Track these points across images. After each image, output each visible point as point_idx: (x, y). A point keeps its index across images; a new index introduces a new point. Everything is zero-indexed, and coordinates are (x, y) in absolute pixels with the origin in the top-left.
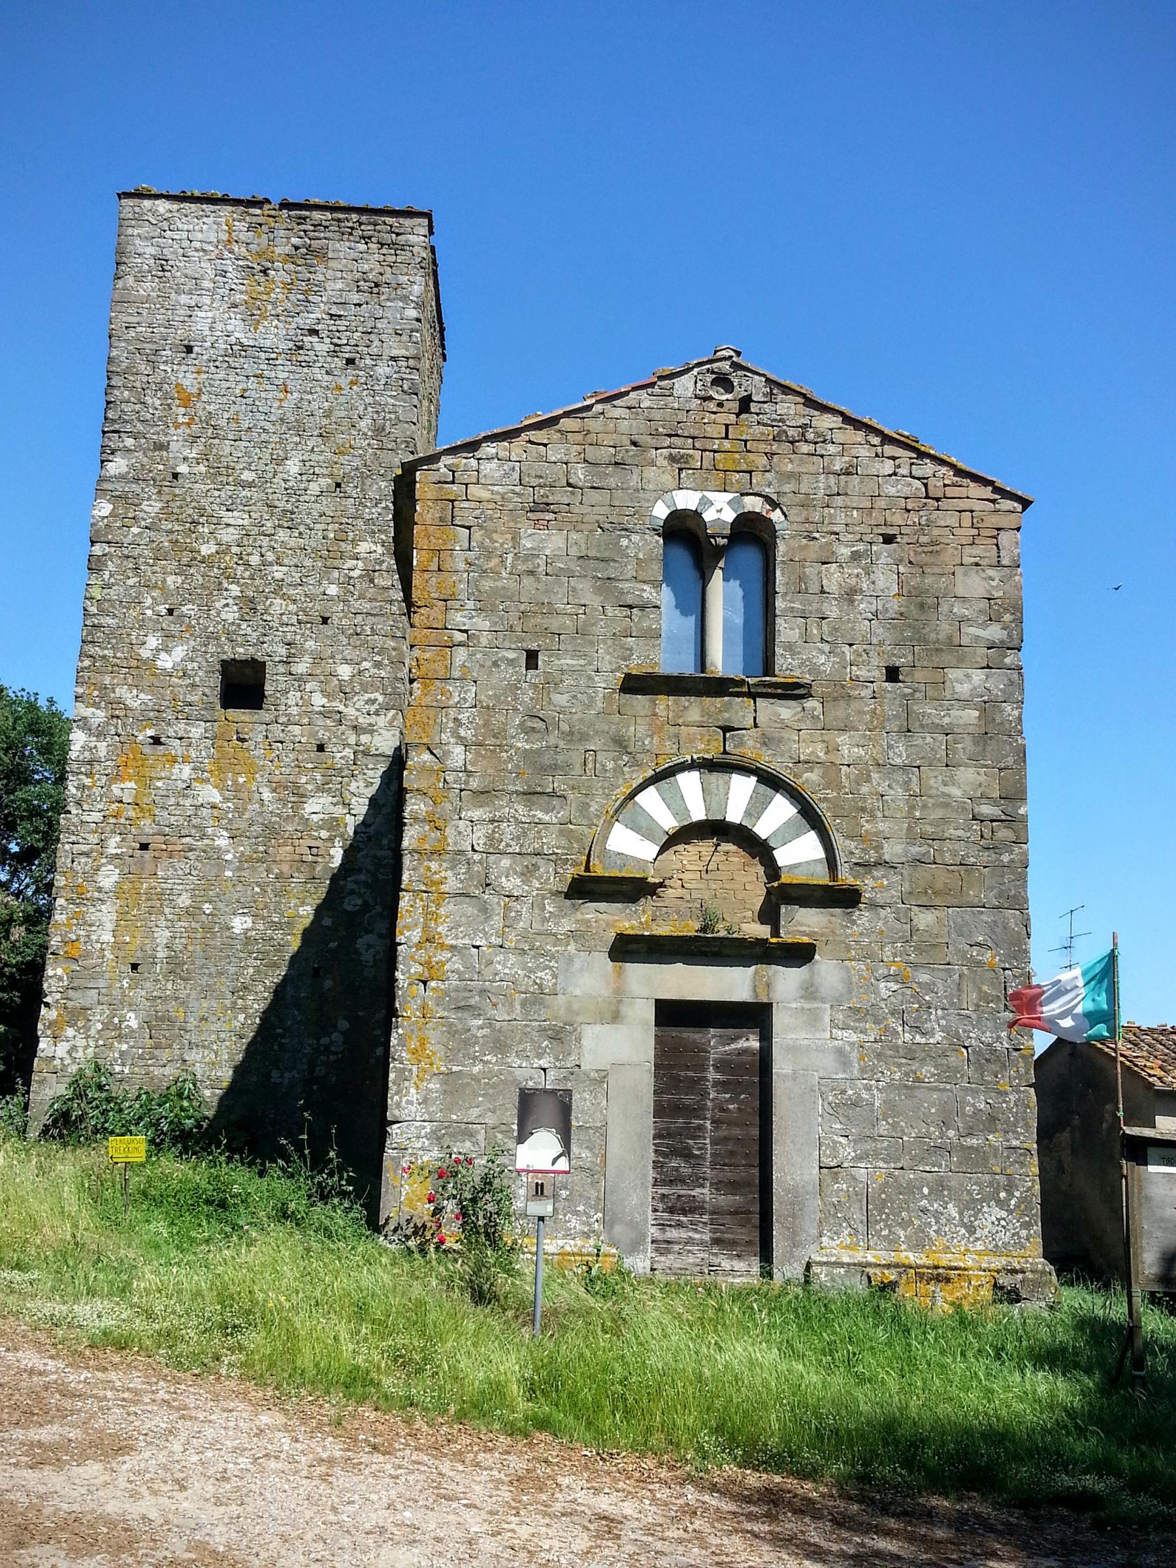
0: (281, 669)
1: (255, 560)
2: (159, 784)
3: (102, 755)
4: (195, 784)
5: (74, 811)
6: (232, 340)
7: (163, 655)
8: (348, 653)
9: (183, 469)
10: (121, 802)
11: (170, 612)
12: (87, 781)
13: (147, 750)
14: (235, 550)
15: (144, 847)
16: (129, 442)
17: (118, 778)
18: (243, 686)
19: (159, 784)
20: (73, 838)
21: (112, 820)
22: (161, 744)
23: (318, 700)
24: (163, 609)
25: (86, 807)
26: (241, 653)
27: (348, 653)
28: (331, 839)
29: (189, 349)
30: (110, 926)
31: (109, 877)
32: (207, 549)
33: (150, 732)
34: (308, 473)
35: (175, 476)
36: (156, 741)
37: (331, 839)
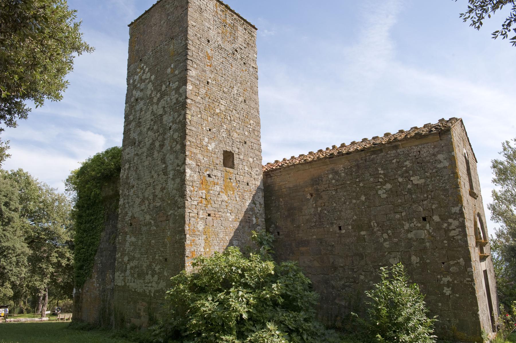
0: (237, 156)
1: (229, 118)
2: (211, 192)
3: (196, 179)
4: (221, 193)
5: (189, 200)
6: (219, 43)
7: (209, 145)
8: (251, 155)
9: (209, 81)
10: (202, 198)
11: (210, 130)
12: (192, 189)
13: (208, 179)
14: (224, 113)
15: (209, 215)
16: (195, 66)
17: (200, 189)
18: (228, 159)
19: (211, 192)
20: (190, 211)
21: (200, 204)
22: (211, 177)
23: (246, 169)
24: (208, 129)
25: (192, 199)
26: (229, 149)
27: (251, 155)
28: (252, 215)
29: (209, 41)
30: (203, 245)
31: (201, 226)
32: (218, 111)
33: (208, 173)
34: (239, 94)
35: (208, 83)
36: (209, 176)
37: (252, 215)
